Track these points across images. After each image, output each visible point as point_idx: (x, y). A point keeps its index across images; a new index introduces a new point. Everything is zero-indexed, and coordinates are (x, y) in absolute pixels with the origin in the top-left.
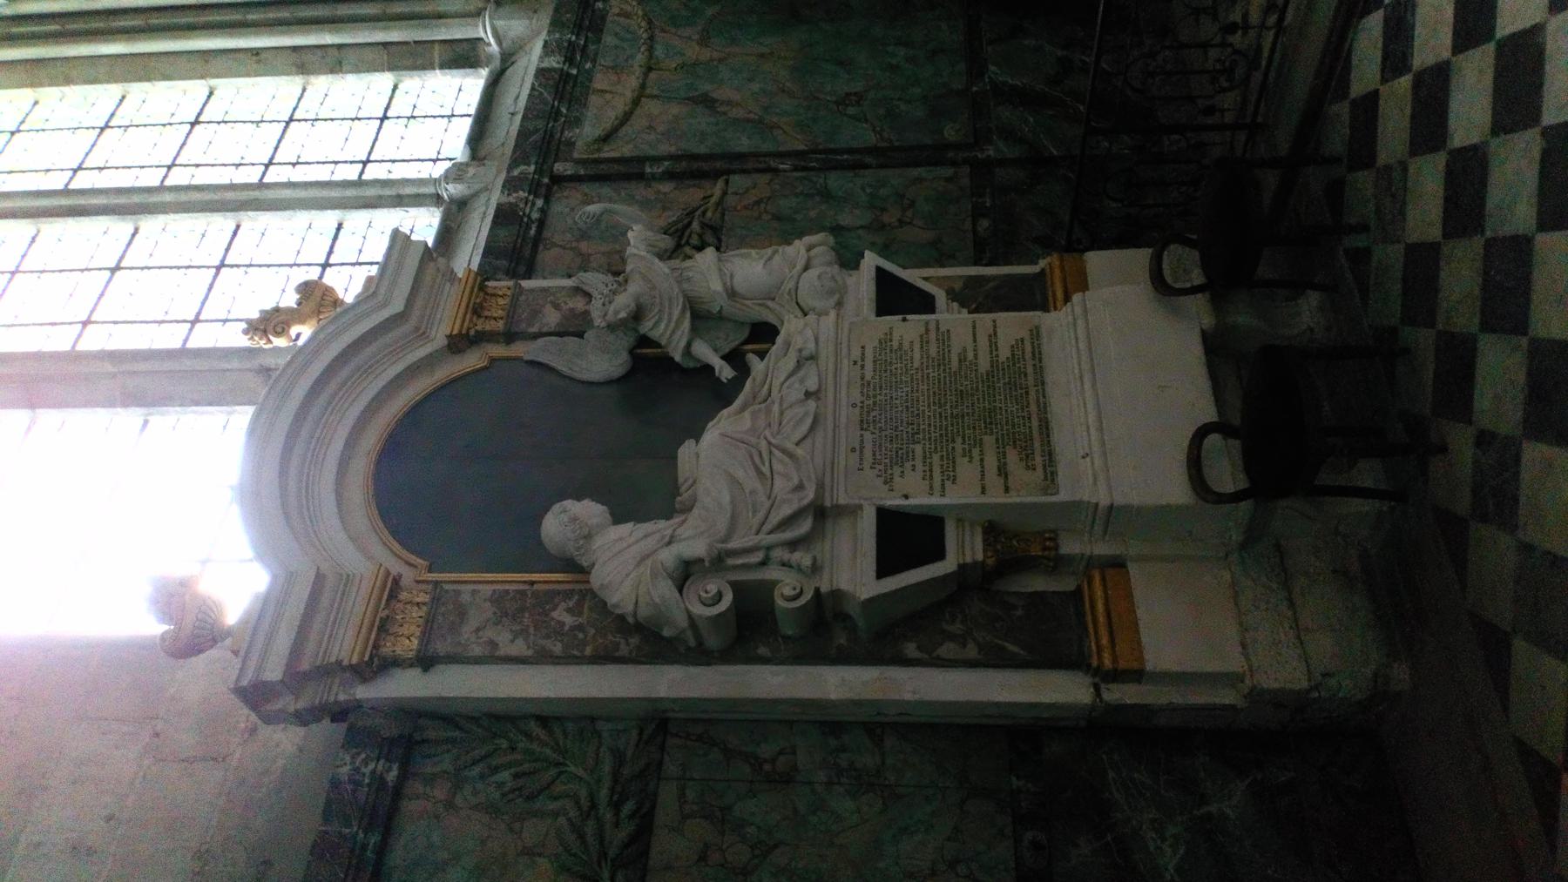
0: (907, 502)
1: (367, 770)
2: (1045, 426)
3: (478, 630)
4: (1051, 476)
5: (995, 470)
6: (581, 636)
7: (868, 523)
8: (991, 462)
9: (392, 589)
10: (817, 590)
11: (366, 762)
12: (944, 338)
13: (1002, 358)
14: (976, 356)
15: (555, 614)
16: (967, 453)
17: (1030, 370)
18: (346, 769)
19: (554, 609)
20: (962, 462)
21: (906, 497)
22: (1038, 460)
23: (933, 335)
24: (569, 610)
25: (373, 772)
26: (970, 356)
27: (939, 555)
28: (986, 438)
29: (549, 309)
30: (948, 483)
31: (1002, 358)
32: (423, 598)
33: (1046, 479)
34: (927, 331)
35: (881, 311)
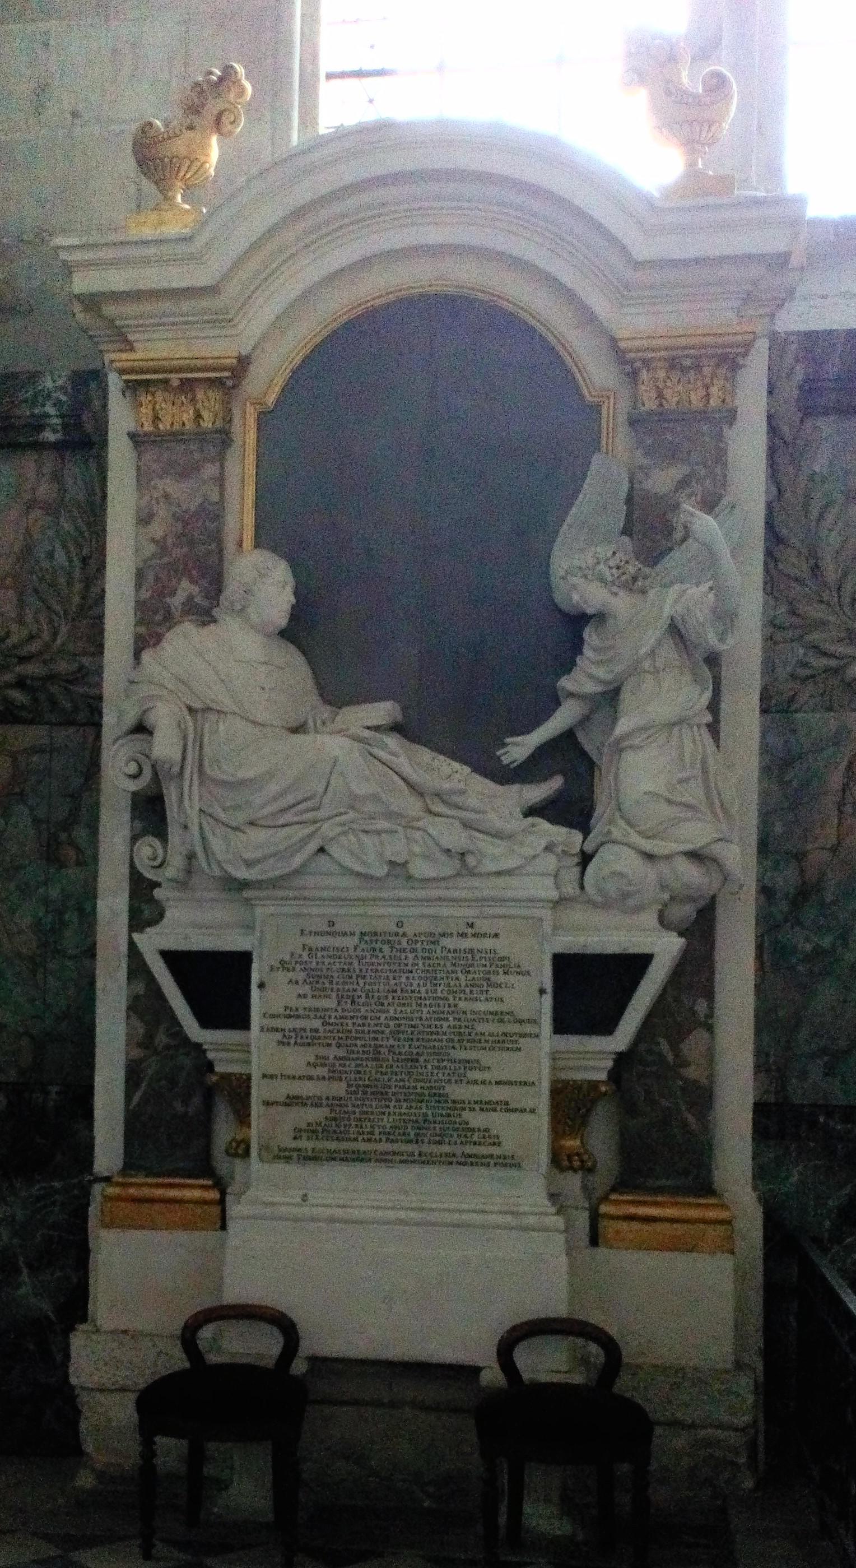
0: (254, 987)
1: (50, 409)
2: (359, 1158)
3: (166, 496)
4: (284, 1155)
6: (158, 618)
7: (235, 942)
8: (307, 1089)
9: (230, 378)
10: (158, 885)
11: (58, 403)
12: (506, 1043)
13: (466, 1115)
14: (476, 1082)
15: (185, 584)
16: (321, 1061)
17: (446, 1149)
18: (49, 384)
20: (309, 1054)
21: (261, 986)
23: (516, 1028)
24: (190, 598)
25: (47, 416)
26: (473, 1075)
27: (206, 1022)
28: (344, 1085)
29: (677, 472)
30: (279, 1036)
31: (466, 1115)
32: (207, 424)
34: (521, 1022)
35: (562, 963)
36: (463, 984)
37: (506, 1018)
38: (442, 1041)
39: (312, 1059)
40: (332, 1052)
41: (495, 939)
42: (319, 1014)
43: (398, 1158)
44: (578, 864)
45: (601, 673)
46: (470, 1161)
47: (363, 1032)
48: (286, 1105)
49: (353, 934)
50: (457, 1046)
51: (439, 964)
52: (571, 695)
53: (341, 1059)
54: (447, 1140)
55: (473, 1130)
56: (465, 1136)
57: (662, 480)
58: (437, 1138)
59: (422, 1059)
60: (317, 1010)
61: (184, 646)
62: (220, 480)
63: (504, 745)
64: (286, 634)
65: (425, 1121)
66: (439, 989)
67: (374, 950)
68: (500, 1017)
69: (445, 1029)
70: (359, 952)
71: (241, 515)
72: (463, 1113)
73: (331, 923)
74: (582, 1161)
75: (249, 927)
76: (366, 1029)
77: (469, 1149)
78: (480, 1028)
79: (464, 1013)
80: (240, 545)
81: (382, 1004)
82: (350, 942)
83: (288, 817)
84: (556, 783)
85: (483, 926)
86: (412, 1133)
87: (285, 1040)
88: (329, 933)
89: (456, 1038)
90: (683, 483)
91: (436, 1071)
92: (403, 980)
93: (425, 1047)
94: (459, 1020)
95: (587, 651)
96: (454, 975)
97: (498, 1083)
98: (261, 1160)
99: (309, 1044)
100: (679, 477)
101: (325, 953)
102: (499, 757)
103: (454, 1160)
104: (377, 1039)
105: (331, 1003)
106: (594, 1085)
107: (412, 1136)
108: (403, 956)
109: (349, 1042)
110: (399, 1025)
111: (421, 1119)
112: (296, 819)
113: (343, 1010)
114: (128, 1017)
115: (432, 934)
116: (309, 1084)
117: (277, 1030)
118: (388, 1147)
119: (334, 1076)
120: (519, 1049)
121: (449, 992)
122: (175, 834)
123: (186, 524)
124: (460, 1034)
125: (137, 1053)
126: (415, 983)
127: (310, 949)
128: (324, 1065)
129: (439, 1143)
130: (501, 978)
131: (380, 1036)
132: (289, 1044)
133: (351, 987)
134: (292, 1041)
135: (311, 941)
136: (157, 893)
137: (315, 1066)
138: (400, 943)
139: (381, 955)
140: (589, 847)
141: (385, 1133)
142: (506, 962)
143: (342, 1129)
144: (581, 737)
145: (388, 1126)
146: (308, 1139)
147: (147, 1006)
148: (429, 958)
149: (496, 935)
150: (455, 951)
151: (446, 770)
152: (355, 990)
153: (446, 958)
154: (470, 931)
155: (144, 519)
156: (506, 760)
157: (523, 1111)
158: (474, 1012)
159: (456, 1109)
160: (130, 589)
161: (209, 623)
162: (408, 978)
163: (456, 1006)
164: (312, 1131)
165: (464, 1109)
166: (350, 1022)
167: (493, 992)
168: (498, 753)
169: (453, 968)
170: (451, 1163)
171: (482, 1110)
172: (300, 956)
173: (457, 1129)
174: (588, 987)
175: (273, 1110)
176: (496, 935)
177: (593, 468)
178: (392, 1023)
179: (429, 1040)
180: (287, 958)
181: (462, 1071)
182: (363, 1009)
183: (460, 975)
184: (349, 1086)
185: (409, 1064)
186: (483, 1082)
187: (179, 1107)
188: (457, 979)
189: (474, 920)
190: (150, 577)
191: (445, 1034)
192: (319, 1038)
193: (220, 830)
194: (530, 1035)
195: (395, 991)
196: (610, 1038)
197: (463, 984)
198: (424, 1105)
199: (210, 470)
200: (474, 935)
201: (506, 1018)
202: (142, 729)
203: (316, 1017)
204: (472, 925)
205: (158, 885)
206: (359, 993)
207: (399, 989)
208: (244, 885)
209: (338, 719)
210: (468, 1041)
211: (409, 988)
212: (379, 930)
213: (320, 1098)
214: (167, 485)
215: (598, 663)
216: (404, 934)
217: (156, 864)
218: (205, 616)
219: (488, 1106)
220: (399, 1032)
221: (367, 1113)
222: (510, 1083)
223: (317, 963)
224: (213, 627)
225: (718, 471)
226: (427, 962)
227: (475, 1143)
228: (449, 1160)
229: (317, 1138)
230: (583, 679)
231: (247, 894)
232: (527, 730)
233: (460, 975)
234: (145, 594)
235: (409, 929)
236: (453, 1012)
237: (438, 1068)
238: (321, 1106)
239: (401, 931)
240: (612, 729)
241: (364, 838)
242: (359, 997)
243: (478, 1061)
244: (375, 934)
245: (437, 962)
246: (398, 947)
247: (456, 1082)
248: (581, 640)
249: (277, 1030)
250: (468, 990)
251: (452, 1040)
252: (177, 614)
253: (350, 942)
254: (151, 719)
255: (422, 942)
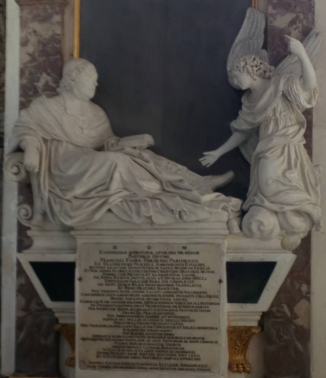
3: (35, 32)
4: (92, 366)
5: (96, 333)
6: (31, 93)
8: (104, 332)
10: (29, 228)
12: (203, 308)
13: (183, 345)
14: (187, 328)
15: (44, 75)
16: (110, 318)
17: (172, 362)
19: (48, 74)
20: (104, 314)
22: (104, 360)
26: (186, 324)
27: (54, 297)
29: (289, 17)
30: (89, 305)
31: (183, 345)
33: (90, 363)
34: (210, 297)
36: (181, 277)
37: (202, 295)
38: (170, 307)
39: (106, 317)
40: (116, 313)
41: (197, 255)
42: (109, 293)
43: (149, 367)
44: (239, 216)
45: (250, 119)
46: (184, 368)
47: (131, 302)
48: (93, 340)
49: (126, 253)
50: (178, 309)
51: (169, 268)
52: (237, 130)
53: (120, 316)
54: (173, 357)
55: (186, 352)
56: (183, 355)
57: (282, 21)
58: (168, 357)
59: (160, 316)
60: (108, 291)
61: (44, 108)
62: (62, 24)
63: (204, 156)
64: (94, 100)
65: (162, 348)
66: (169, 280)
67: (137, 260)
68: (199, 294)
69: (172, 301)
70: (129, 262)
71: (73, 41)
72: (181, 343)
73: (115, 247)
74: (244, 368)
75: (74, 250)
76: (132, 301)
77: (185, 362)
78: (190, 300)
79: (182, 292)
80: (72, 55)
81: (140, 288)
82: (125, 257)
83: (93, 194)
84: (229, 176)
85: (191, 248)
86: (156, 354)
87: (92, 307)
88: (113, 253)
89: (178, 305)
90: (292, 22)
91: (167, 322)
92: (151, 276)
93: (162, 310)
94: (179, 296)
95: (243, 108)
96: (177, 274)
97: (199, 328)
98: (81, 368)
99: (104, 309)
100: (290, 19)
101: (112, 263)
102: (200, 162)
103: (177, 367)
104: (138, 306)
105: (115, 288)
106: (249, 329)
107: (156, 356)
108: (151, 263)
109: (124, 307)
110: (149, 299)
111: (160, 347)
112: (97, 195)
113: (121, 292)
114: (17, 295)
115: (166, 253)
116: (103, 329)
117: (87, 302)
118: (143, 361)
119: (117, 325)
120: (209, 311)
121: (174, 282)
122: (38, 204)
123: (44, 45)
124: (180, 303)
125: (22, 314)
126: (157, 277)
127: (104, 260)
128: (112, 319)
129: (169, 359)
130: (200, 275)
131: (139, 304)
132: (94, 309)
133: (124, 280)
134: (96, 308)
135: (103, 256)
136: (29, 233)
137: (107, 320)
138: (149, 257)
139: (139, 263)
140: (245, 207)
141: (142, 354)
142: (203, 266)
143: (121, 352)
144: (243, 151)
145: (144, 350)
146: (104, 357)
147: (25, 290)
148: (164, 265)
149: (197, 253)
150: (177, 261)
151: (174, 169)
152: (127, 281)
153: (172, 265)
154: (184, 251)
155: (24, 43)
156: (204, 163)
157: (211, 342)
158: (186, 292)
159: (178, 341)
160: (17, 78)
161: (54, 95)
162: (153, 275)
163: (177, 289)
164: (106, 353)
165: (182, 341)
166: (124, 298)
167: (196, 282)
168: (200, 160)
169: (176, 270)
170: (175, 369)
171: (191, 342)
172: (99, 264)
173: (179, 352)
174: (244, 280)
175: (87, 342)
176: (197, 253)
177: (248, 15)
178: (145, 298)
179: (165, 306)
180: (93, 265)
181: (181, 322)
182: (131, 291)
183: (179, 273)
184: (125, 330)
185: (154, 319)
186: (191, 328)
187: (43, 341)
188: (178, 275)
189: (186, 245)
190: (27, 73)
191: (172, 303)
192: (109, 306)
193: (57, 200)
194: (215, 304)
195: (147, 282)
196: (256, 304)
197: (181, 277)
198: (162, 340)
199: (57, 18)
200: (186, 253)
201: (202, 295)
202: (19, 150)
203: (107, 295)
204: (185, 248)
205: (29, 228)
206: (129, 283)
207: (149, 280)
208: (71, 229)
209: (120, 143)
210: (184, 307)
211: (154, 280)
212: (139, 250)
213: (110, 336)
214: (36, 26)
215: (248, 114)
216: (151, 253)
217: (27, 218)
218: (52, 91)
219: (194, 340)
220: (149, 302)
221: (133, 344)
222: (205, 328)
223: (108, 268)
224: (57, 98)
225: (310, 16)
226: (163, 267)
227: (187, 359)
228: (173, 368)
229: (108, 357)
230: (241, 123)
231: (72, 233)
232: (214, 148)
233: (179, 273)
234: (25, 81)
235: (154, 250)
236: (176, 292)
237: (169, 320)
238: (110, 340)
239: (150, 251)
240: (254, 148)
241: (130, 204)
242: (129, 285)
243: (189, 318)
244: (137, 253)
245: (168, 266)
246: (149, 259)
247: (178, 328)
248: (240, 104)
249: (87, 302)
250: (183, 281)
251: (176, 307)
252: (40, 91)
253: (125, 257)
254: (23, 145)
255: (160, 256)
